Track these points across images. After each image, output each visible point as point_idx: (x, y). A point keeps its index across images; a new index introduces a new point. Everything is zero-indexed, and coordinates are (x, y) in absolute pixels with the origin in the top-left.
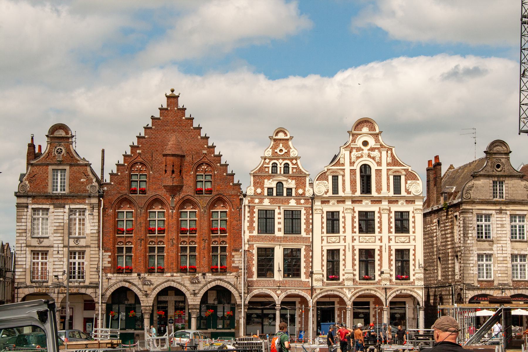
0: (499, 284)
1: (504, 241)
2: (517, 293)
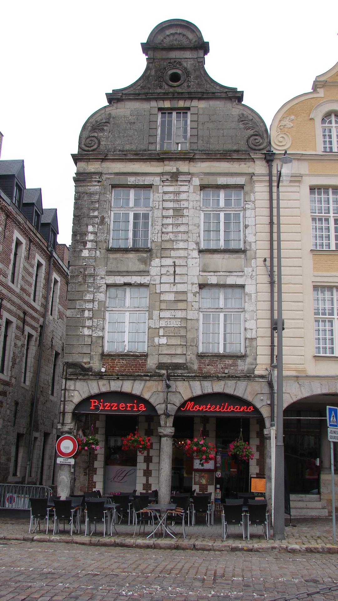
0: (161, 366)
1: (181, 251)
2: (210, 391)
